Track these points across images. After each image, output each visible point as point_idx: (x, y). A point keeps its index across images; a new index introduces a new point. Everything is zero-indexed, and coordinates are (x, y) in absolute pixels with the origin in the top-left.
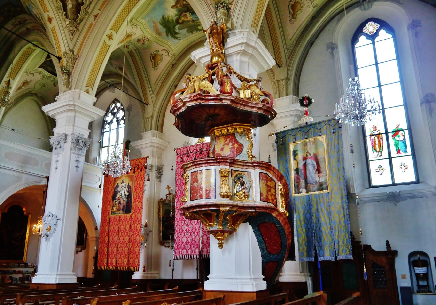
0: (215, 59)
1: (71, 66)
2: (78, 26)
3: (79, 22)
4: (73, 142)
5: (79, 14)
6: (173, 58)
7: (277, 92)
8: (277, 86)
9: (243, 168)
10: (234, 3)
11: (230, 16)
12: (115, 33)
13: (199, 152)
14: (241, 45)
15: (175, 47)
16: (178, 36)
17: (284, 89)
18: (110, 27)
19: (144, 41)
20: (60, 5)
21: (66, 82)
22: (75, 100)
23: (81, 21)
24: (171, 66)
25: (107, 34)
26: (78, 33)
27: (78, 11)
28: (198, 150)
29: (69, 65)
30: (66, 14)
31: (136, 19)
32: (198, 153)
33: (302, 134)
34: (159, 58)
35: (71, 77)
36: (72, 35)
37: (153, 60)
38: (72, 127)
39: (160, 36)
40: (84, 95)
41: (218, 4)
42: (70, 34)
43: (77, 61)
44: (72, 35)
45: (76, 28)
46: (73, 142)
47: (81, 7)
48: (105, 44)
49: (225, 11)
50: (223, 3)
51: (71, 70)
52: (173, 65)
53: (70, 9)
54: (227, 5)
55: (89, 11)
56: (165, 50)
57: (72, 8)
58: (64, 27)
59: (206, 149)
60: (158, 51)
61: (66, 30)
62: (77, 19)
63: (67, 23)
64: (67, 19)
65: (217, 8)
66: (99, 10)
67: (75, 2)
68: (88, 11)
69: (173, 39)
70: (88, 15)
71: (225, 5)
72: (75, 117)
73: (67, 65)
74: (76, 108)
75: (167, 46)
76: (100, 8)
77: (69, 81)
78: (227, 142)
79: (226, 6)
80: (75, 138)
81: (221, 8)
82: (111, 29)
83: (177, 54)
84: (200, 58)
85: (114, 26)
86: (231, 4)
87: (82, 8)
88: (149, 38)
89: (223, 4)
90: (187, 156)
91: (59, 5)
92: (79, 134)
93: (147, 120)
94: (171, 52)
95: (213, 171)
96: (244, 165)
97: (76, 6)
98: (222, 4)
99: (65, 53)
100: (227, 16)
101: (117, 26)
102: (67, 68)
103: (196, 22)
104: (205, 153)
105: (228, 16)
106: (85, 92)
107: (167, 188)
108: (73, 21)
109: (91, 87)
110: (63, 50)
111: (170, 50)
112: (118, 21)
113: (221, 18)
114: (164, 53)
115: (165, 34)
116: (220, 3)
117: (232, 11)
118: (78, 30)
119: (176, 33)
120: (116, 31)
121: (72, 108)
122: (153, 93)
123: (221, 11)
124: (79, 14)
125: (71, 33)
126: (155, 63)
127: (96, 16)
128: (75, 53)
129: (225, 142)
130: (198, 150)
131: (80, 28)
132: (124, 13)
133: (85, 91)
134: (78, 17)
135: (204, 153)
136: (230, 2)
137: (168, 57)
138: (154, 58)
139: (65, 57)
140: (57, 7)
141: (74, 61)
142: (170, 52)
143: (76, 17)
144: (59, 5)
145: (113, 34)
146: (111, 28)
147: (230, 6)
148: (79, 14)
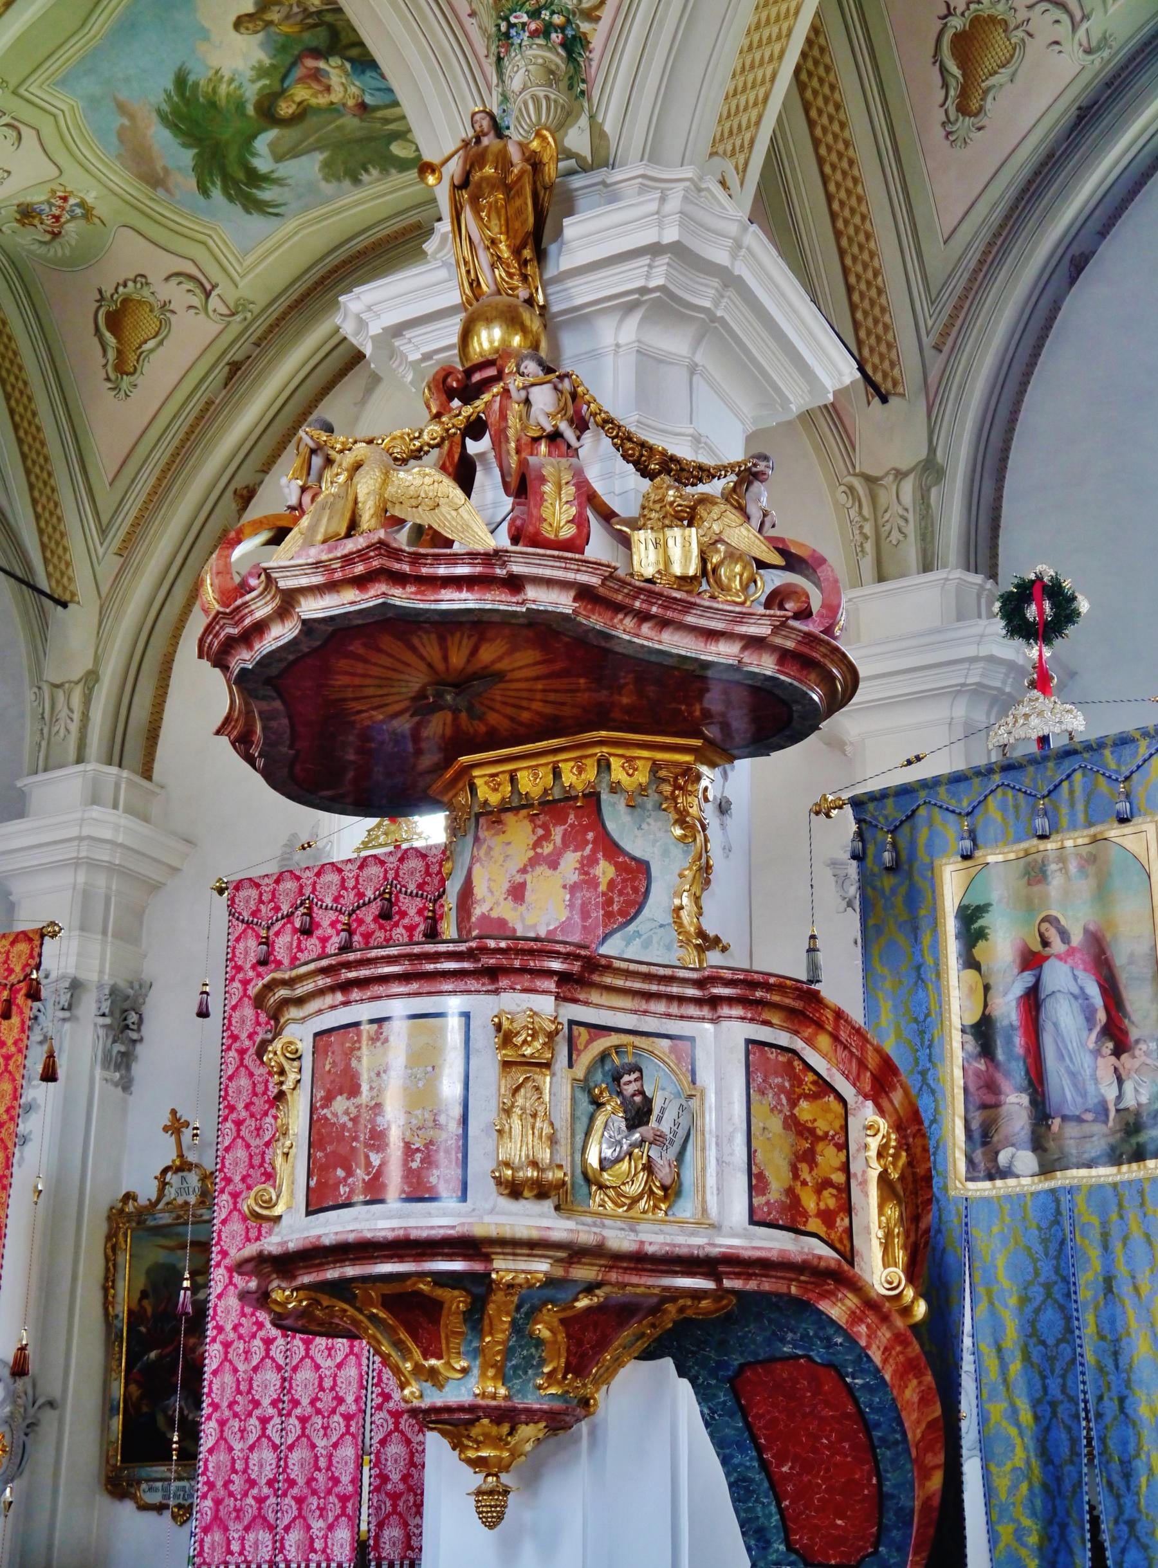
0: (484, 334)
6: (235, 328)
7: (869, 546)
8: (866, 511)
9: (645, 1012)
10: (607, 13)
11: (583, 86)
13: (375, 909)
14: (646, 260)
15: (249, 260)
16: (267, 194)
17: (911, 529)
19: (57, 218)
24: (221, 372)
28: (370, 894)
32: (369, 915)
33: (1016, 807)
34: (149, 324)
37: (108, 335)
39: (160, 192)
41: (512, 11)
49: (557, 59)
52: (235, 368)
54: (568, 21)
56: (191, 277)
59: (420, 886)
60: (141, 279)
65: (507, 35)
69: (237, 210)
71: (558, 20)
75: (200, 254)
78: (547, 849)
79: (562, 29)
81: (534, 34)
83: (262, 300)
84: (398, 330)
86: (591, 16)
88: (90, 200)
89: (545, 14)
90: (295, 931)
93: (60, 696)
94: (224, 288)
95: (454, 1024)
96: (648, 996)
98: (535, 14)
100: (563, 85)
103: (379, 114)
104: (412, 912)
105: (571, 87)
107: (166, 1129)
111: (216, 275)
113: (526, 95)
114: (179, 295)
115: (193, 182)
117: (595, 56)
119: (255, 178)
122: (103, 532)
126: (120, 353)
129: (537, 844)
130: (370, 894)
135: (403, 914)
137: (202, 316)
138: (115, 322)
142: (214, 287)
147: (585, 27)
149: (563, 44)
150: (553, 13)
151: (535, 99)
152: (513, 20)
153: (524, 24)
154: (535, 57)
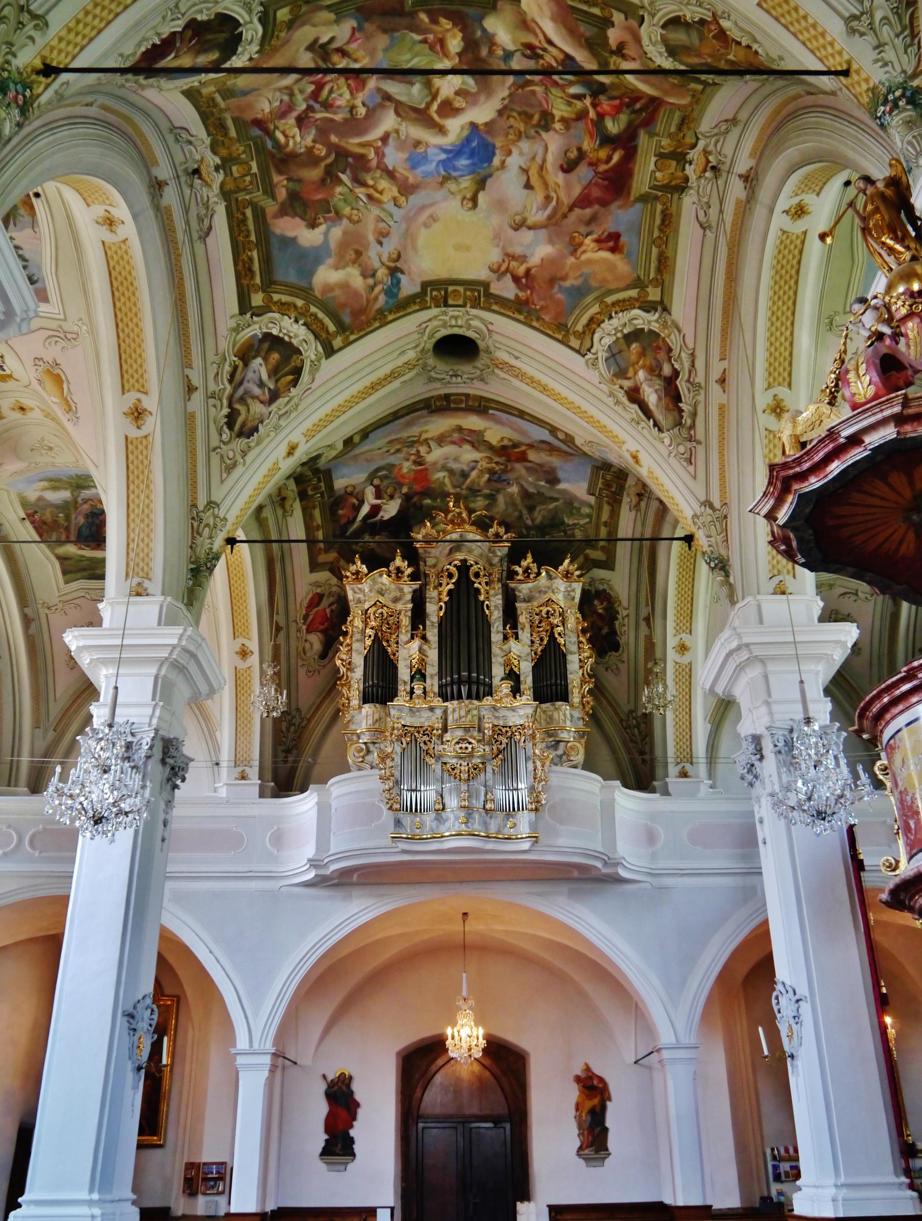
1: (720, 544)
2: (692, 432)
3: (689, 422)
4: (780, 752)
5: (680, 405)
12: (786, 390)
18: (760, 383)
20: (636, 412)
21: (725, 590)
22: (739, 630)
23: (694, 415)
25: (764, 407)
26: (701, 450)
27: (676, 398)
29: (714, 545)
30: (656, 424)
31: (840, 309)
35: (731, 572)
36: (691, 464)
38: (763, 710)
40: (773, 606)
42: (685, 464)
43: (728, 520)
44: (691, 464)
45: (690, 441)
46: (780, 752)
47: (678, 382)
48: (771, 436)
50: (888, 93)
51: (723, 552)
53: (657, 406)
54: (905, 89)
55: (700, 378)
57: (660, 399)
58: (666, 457)
61: (673, 461)
62: (682, 417)
63: (667, 441)
64: (663, 432)
66: (722, 359)
67: (658, 382)
68: (697, 380)
70: (702, 392)
71: (898, 93)
72: (766, 678)
73: (710, 546)
74: (757, 651)
76: (722, 353)
77: (730, 585)
79: (903, 95)
80: (781, 739)
82: (769, 386)
85: (770, 374)
87: (681, 384)
89: (891, 97)
91: (633, 411)
92: (791, 723)
97: (665, 389)
98: (885, 103)
99: (695, 516)
101: (781, 370)
102: (712, 552)
106: (775, 593)
108: (676, 430)
109: (788, 572)
110: (689, 513)
112: (777, 354)
116: (880, 102)
118: (699, 442)
120: (786, 384)
121: (744, 655)
123: (894, 123)
124: (681, 402)
125: (686, 460)
127: (722, 381)
128: (717, 505)
131: (700, 433)
132: (779, 324)
133: (772, 591)
134: (683, 411)
136: (910, 72)
139: (699, 528)
140: (633, 420)
141: (721, 526)
143: (676, 413)
144: (633, 411)
145: (781, 397)
146: (766, 386)
148: (681, 402)
149: (908, 103)
150: (894, 92)
151: (910, 143)
152: (879, 115)
153: (884, 112)
154: (897, 122)
